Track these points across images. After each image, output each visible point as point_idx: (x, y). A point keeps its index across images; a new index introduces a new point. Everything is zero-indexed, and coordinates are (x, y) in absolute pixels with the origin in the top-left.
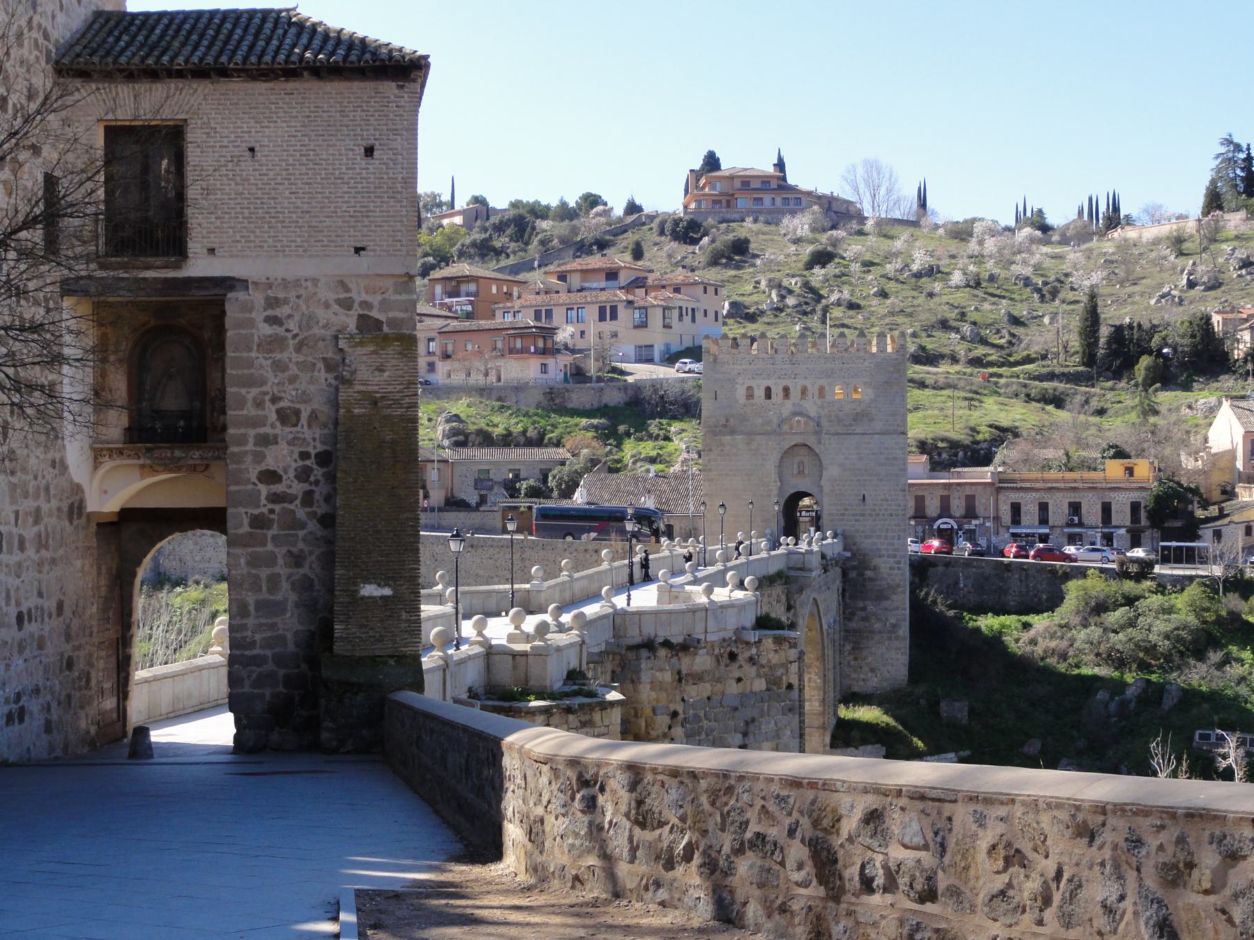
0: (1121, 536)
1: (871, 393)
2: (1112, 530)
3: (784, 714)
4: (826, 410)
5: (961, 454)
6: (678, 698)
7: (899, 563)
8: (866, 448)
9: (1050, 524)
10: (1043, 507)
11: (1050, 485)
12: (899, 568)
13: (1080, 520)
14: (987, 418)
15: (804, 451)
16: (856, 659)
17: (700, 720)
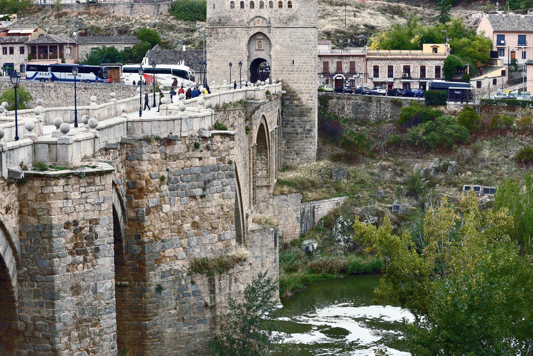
3: (226, 178)
5: (349, 40)
6: (165, 169)
7: (312, 97)
9: (394, 77)
10: (390, 69)
12: (311, 100)
13: (409, 75)
14: (364, 22)
16: (288, 148)
17: (178, 182)
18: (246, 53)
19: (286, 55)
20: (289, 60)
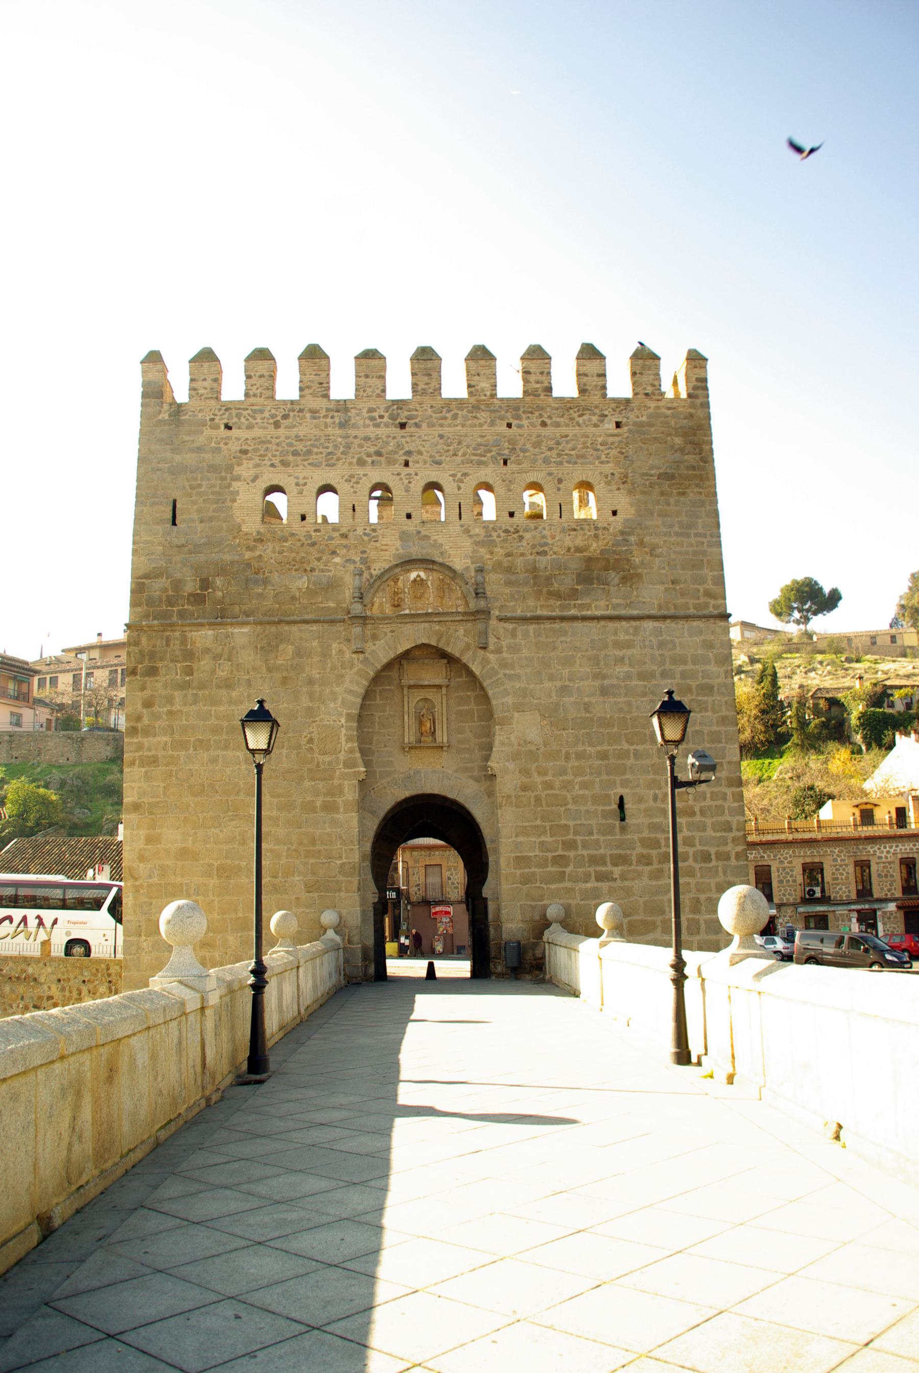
0: (888, 916)
1: (623, 501)
2: (876, 906)
4: (499, 551)
8: (621, 660)
11: (769, 837)
15: (434, 674)
18: (349, 764)
19: (579, 772)
20: (597, 799)
